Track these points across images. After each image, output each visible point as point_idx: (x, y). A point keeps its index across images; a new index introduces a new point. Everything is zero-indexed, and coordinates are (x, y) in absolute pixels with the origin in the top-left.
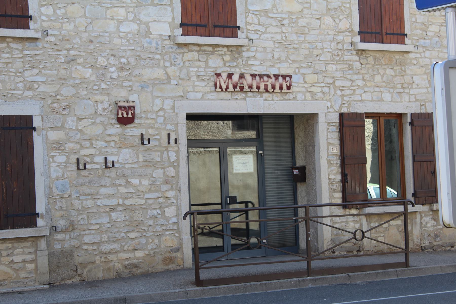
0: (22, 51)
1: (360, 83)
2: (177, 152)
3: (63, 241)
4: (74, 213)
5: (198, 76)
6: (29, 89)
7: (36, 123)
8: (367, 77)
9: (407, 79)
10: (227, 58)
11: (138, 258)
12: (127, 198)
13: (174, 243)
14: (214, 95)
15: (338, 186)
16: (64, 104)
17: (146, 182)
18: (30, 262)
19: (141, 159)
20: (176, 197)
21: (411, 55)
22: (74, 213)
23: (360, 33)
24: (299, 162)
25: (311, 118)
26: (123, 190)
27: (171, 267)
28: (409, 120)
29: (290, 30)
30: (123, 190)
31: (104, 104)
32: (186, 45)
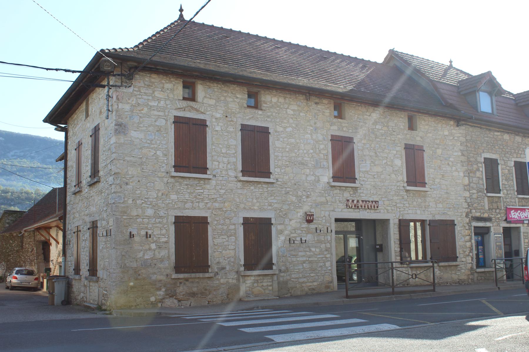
0: (267, 188)
1: (407, 205)
2: (331, 236)
3: (284, 277)
4: (288, 264)
5: (340, 201)
6: (270, 206)
7: (273, 221)
8: (410, 202)
9: (427, 204)
10: (351, 193)
11: (315, 286)
12: (310, 257)
13: (330, 279)
14: (346, 210)
15: (398, 254)
16: (284, 213)
17: (318, 250)
18: (270, 286)
19: (316, 239)
20: (330, 257)
21: (429, 193)
22: (288, 264)
23: (407, 182)
24: (378, 242)
25: (385, 222)
26: (308, 253)
27: (328, 290)
28: (428, 223)
29: (377, 180)
30: (308, 253)
31: (301, 213)
32: (334, 186)
